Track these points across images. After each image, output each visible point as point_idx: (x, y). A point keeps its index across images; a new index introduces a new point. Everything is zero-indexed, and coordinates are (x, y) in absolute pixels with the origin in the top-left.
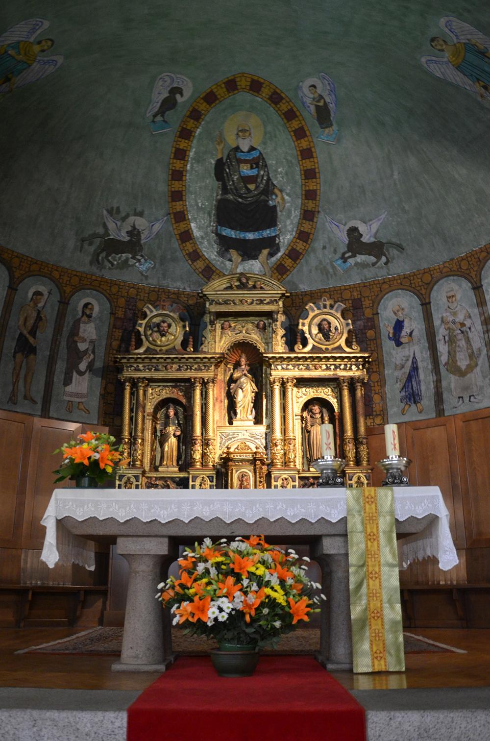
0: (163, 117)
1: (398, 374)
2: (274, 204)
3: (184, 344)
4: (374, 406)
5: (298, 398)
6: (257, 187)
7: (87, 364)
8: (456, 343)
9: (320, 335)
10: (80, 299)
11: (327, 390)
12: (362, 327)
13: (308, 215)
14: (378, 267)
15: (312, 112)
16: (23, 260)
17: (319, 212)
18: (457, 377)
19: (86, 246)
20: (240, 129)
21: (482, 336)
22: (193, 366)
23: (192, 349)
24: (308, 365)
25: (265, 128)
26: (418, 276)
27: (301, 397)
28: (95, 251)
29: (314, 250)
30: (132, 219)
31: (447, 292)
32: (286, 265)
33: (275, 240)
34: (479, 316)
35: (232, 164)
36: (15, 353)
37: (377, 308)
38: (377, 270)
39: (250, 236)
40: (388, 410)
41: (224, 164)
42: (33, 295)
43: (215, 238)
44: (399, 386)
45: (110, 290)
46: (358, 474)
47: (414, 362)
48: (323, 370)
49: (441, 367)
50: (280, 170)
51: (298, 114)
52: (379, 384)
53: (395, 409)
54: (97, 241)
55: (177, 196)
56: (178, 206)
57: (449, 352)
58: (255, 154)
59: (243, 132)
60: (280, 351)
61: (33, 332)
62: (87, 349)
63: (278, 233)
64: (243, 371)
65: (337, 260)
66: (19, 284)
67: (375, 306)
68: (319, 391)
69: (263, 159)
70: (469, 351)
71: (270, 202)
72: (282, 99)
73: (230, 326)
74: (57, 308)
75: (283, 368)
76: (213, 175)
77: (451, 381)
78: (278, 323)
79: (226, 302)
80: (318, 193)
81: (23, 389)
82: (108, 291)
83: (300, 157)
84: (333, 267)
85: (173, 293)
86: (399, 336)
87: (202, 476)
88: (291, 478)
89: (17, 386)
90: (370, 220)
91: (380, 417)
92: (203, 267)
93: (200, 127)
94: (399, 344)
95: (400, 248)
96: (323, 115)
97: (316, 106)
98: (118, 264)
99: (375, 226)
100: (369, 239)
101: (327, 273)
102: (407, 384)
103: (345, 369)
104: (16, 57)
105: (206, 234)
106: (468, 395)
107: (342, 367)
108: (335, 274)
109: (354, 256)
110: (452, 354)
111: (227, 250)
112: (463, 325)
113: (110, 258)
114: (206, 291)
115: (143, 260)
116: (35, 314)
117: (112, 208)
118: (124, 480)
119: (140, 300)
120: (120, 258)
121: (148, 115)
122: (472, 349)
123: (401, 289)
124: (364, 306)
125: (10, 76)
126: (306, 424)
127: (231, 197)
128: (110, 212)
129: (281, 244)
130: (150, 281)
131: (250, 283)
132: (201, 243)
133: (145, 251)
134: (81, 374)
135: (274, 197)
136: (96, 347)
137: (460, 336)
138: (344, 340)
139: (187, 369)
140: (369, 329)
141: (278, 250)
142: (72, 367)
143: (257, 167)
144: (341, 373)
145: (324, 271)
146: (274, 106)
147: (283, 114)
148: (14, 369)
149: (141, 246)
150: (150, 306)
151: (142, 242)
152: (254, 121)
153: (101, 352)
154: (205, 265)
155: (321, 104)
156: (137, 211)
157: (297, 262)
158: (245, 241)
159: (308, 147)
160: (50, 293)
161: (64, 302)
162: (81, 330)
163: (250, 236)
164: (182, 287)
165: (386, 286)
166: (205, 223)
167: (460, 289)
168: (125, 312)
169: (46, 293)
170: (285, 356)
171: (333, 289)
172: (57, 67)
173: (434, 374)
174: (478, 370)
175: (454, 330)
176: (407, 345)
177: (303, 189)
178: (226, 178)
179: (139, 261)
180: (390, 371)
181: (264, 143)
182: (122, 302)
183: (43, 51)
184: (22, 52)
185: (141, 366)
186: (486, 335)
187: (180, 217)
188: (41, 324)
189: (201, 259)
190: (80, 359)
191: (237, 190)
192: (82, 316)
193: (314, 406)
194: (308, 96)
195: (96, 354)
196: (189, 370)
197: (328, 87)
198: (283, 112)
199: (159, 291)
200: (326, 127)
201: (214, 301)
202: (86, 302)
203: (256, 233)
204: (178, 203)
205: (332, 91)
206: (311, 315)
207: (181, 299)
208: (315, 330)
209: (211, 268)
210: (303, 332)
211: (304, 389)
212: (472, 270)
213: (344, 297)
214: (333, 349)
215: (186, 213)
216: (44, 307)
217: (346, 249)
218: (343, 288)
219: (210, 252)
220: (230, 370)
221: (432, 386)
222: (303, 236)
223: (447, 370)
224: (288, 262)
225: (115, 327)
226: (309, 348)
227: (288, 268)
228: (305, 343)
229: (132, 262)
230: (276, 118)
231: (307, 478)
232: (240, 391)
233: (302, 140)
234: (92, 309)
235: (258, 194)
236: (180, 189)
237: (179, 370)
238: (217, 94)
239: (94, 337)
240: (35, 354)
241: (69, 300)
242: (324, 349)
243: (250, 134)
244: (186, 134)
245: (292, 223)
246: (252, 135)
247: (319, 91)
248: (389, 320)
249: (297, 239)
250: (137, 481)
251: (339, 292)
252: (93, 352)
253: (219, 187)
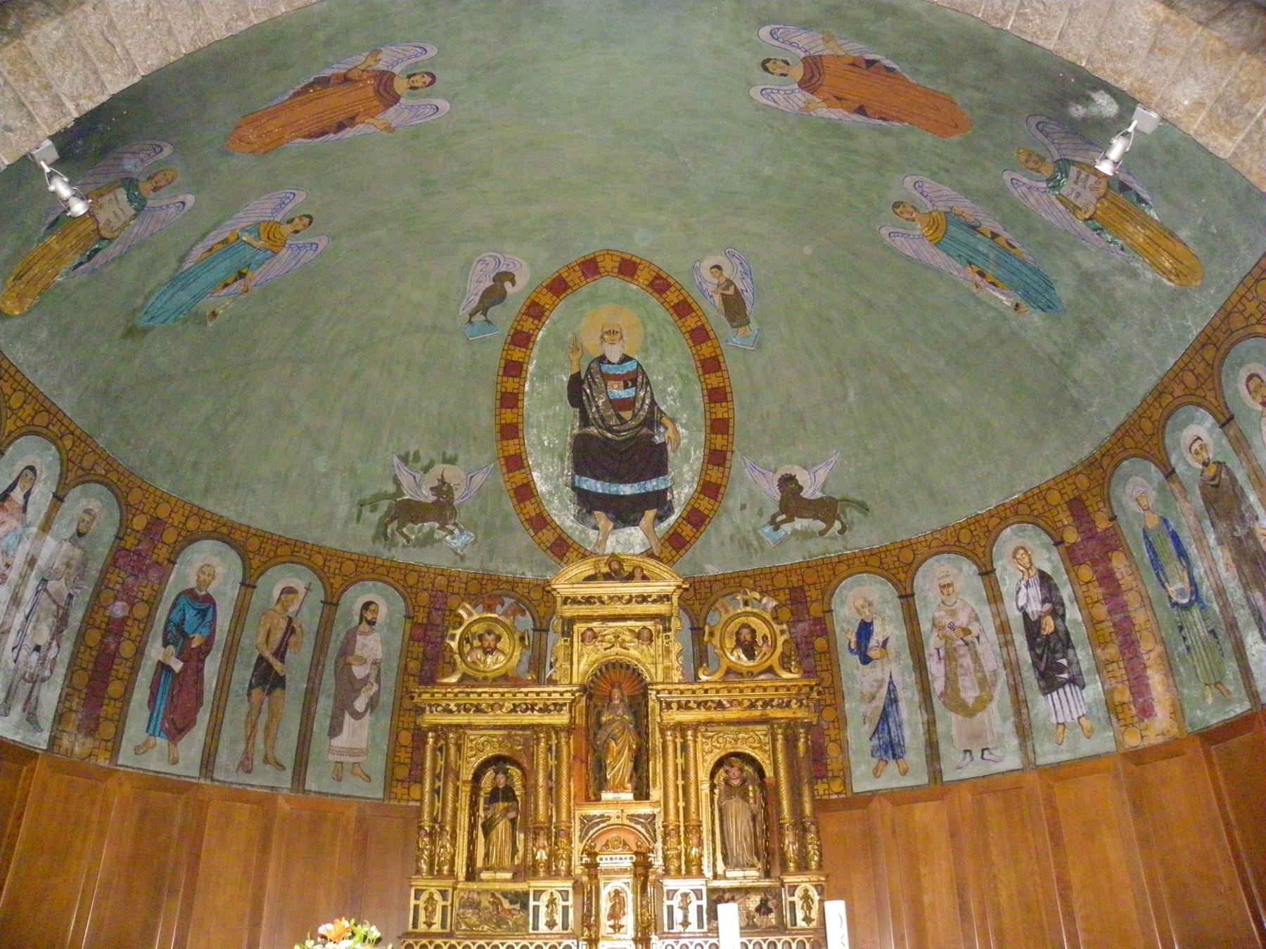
0: (485, 315)
1: (864, 708)
2: (663, 440)
4: (829, 761)
5: (705, 755)
6: (635, 416)
7: (367, 700)
8: (956, 660)
10: (357, 597)
12: (806, 633)
13: (716, 458)
14: (830, 538)
15: (717, 303)
16: (265, 540)
17: (733, 452)
18: (960, 717)
19: (366, 512)
20: (605, 330)
21: (998, 650)
22: (536, 704)
25: (645, 327)
26: (894, 553)
28: (381, 519)
29: (726, 511)
30: (438, 468)
31: (939, 579)
32: (684, 534)
33: (666, 496)
34: (991, 618)
35: (594, 382)
36: (251, 687)
37: (830, 603)
38: (828, 541)
39: (627, 490)
40: (853, 768)
41: (582, 382)
42: (281, 594)
43: (572, 494)
44: (868, 729)
45: (405, 580)
47: (892, 689)
48: (745, 709)
49: (935, 700)
50: (669, 389)
51: (695, 306)
52: (836, 724)
53: (863, 768)
54: (384, 505)
55: (510, 431)
56: (512, 447)
57: (946, 676)
58: (630, 367)
59: (611, 334)
61: (280, 654)
62: (368, 676)
63: (669, 485)
65: (764, 526)
66: (258, 578)
67: (826, 600)
69: (644, 373)
70: (979, 675)
71: (657, 437)
72: (669, 286)
74: (319, 613)
76: (566, 398)
77: (950, 724)
80: (731, 425)
81: (262, 746)
82: (402, 582)
83: (700, 370)
84: (759, 538)
85: (507, 582)
86: (866, 648)
87: (550, 890)
89: (254, 743)
90: (813, 465)
91: (839, 781)
92: (552, 540)
93: (544, 329)
94: (866, 660)
95: (863, 508)
96: (735, 308)
97: (722, 295)
98: (417, 539)
99: (822, 474)
100: (813, 494)
101: (749, 545)
102: (880, 726)
103: (779, 706)
104: (255, 243)
105: (557, 487)
106: (980, 748)
108: (762, 549)
109: (790, 520)
110: (950, 680)
111: (590, 512)
112: (967, 631)
113: (404, 530)
115: (457, 532)
116: (284, 624)
117: (407, 454)
118: (424, 896)
119: (453, 594)
120: (420, 530)
121: (461, 313)
122: (983, 671)
123: (866, 572)
124: (809, 599)
125: (244, 271)
127: (593, 430)
128: (404, 459)
129: (675, 502)
130: (468, 563)
131: (626, 568)
132: (550, 502)
133: (462, 513)
134: (357, 716)
135: (662, 430)
136: (382, 671)
137: (963, 650)
139: (527, 710)
140: (818, 636)
141: (671, 510)
142: (343, 705)
143: (634, 384)
145: (745, 545)
146: (657, 296)
147: (673, 307)
148: (249, 714)
149: (454, 508)
150: (468, 606)
151: (455, 503)
152: (626, 318)
153: (389, 681)
154: (556, 536)
155: (731, 291)
156: (448, 456)
157: (701, 530)
158: (618, 498)
159: (713, 354)
160: (308, 589)
161: (331, 603)
162: (358, 646)
163: (627, 490)
164: (520, 571)
165: (843, 567)
166: (554, 470)
167: (963, 572)
168: (429, 614)
169: (302, 590)
171: (758, 572)
172: (318, 252)
173: (923, 711)
174: (993, 706)
175: (953, 640)
176: (879, 661)
177: (708, 417)
178: (586, 402)
179: (451, 533)
180: (854, 705)
181: (645, 350)
182: (424, 598)
183: (296, 232)
184: (264, 236)
186: (1005, 649)
187: (515, 463)
188: (293, 639)
189: (548, 527)
190: (358, 691)
191: (603, 420)
192: (360, 623)
194: (711, 282)
195: (382, 682)
196: (529, 712)
197: (740, 268)
198: (672, 304)
199: (483, 579)
200: (741, 326)
201: (569, 598)
202: (367, 600)
203: (636, 485)
204: (511, 442)
205: (747, 273)
207: (518, 590)
208: (729, 643)
209: (565, 541)
212: (977, 546)
213: (778, 585)
215: (524, 457)
216: (298, 612)
217: (778, 509)
218: (774, 570)
219: (564, 515)
221: (921, 730)
222: (711, 490)
223: (944, 703)
224: (687, 530)
225: (411, 638)
227: (688, 539)
229: (438, 534)
230: (662, 313)
232: (613, 744)
233: (704, 345)
234: (376, 612)
235: (637, 427)
236: (514, 421)
237: (514, 710)
238: (567, 279)
239: (379, 655)
240: (284, 687)
241: (338, 600)
243: (622, 337)
244: (521, 339)
245: (691, 469)
246: (625, 338)
247: (727, 273)
248: (849, 622)
249: (700, 493)
250: (445, 899)
251: (768, 576)
252: (378, 680)
253: (575, 416)
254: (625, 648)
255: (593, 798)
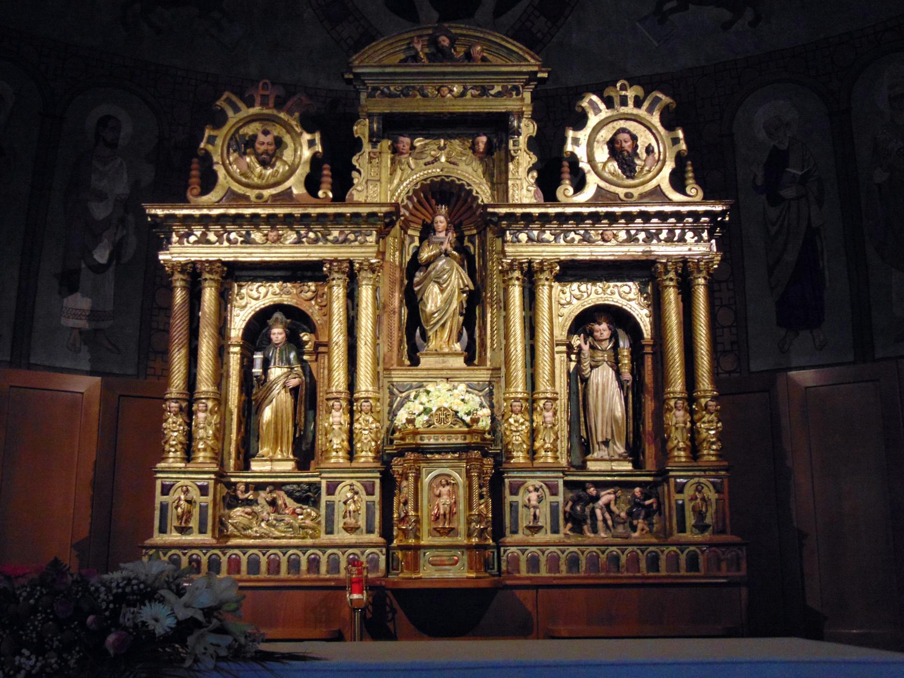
3: (312, 184)
9: (614, 166)
11: (626, 289)
23: (331, 195)
24: (586, 231)
27: (569, 303)
46: (696, 480)
48: (621, 244)
60: (526, 201)
64: (442, 243)
68: (609, 291)
73: (413, 148)
75: (530, 239)
78: (523, 140)
79: (405, 93)
87: (348, 482)
88: (546, 484)
103: (669, 240)
107: (664, 235)
114: (359, 67)
126: (579, 362)
138: (668, 175)
144: (660, 249)
170: (536, 211)
185: (212, 237)
193: (600, 324)
196: (320, 244)
206: (593, 120)
208: (602, 154)
210: (573, 160)
211: (575, 285)
214: (642, 196)
220: (412, 241)
226: (588, 193)
228: (579, 184)
231: (582, 485)
242: (622, 196)
254: (454, 164)
255: (407, 362)
